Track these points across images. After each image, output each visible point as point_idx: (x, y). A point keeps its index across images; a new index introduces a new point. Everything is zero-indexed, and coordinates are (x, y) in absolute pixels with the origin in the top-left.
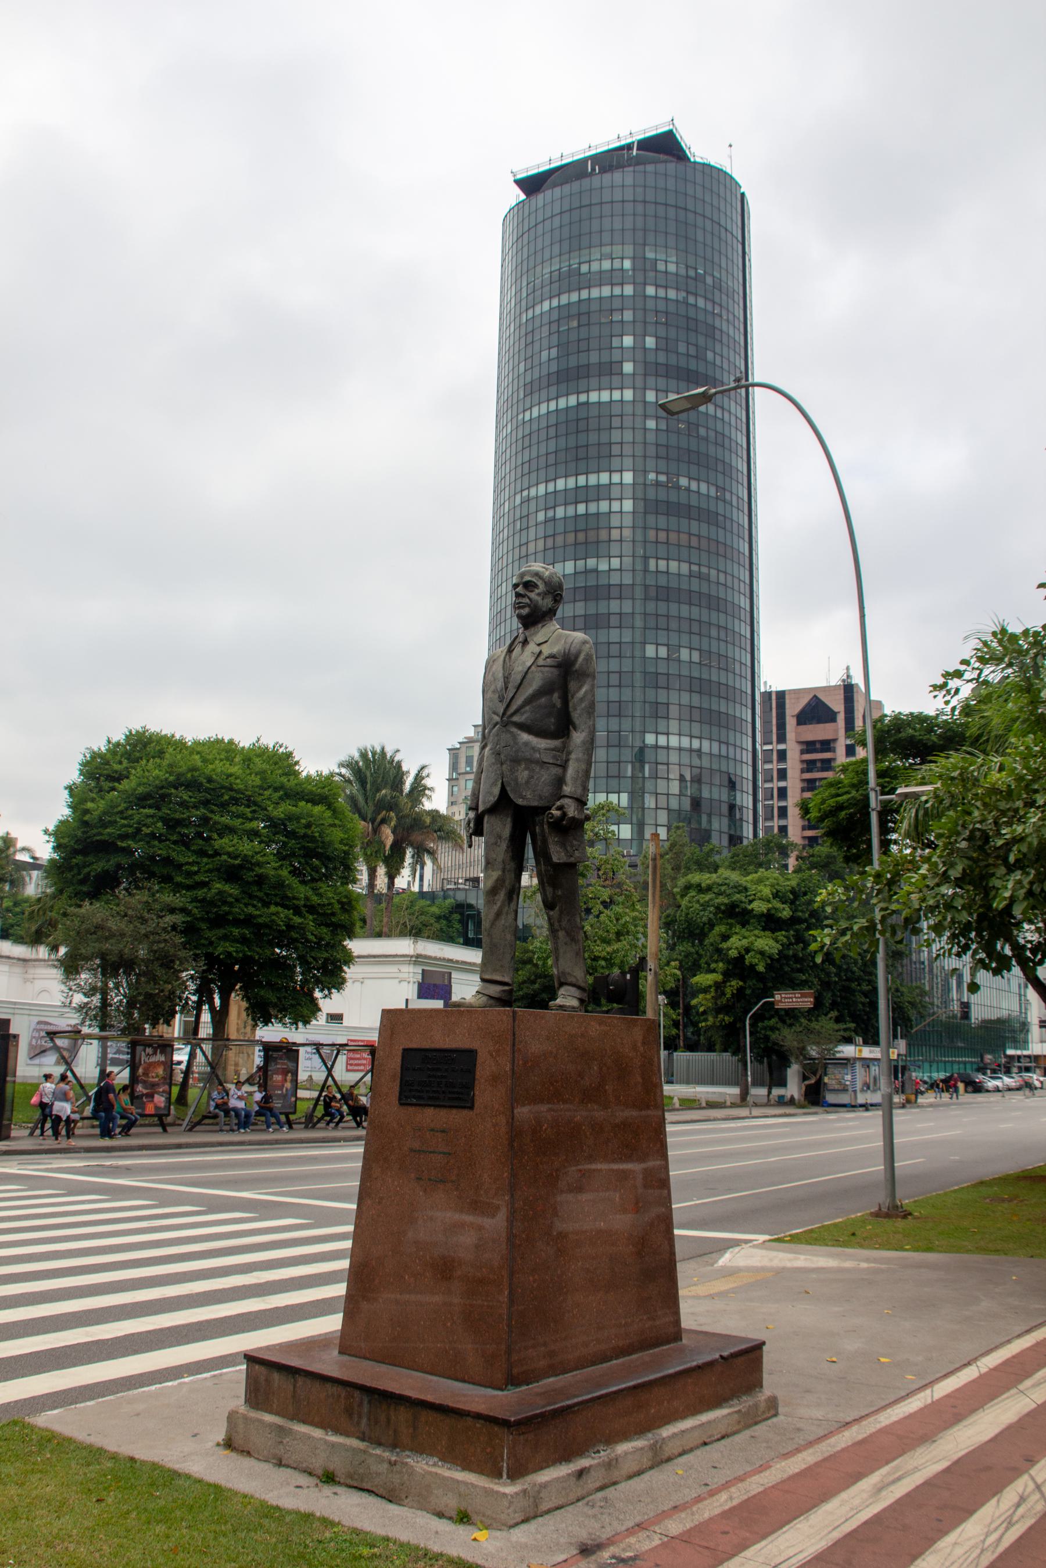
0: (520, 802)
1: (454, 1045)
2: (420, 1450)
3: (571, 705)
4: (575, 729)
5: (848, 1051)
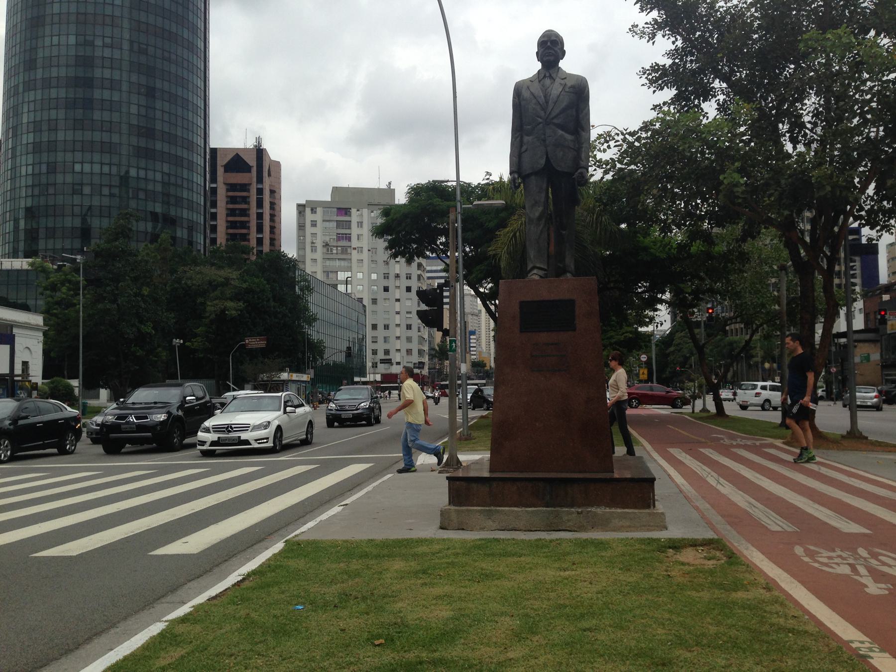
0: (559, 169)
1: (557, 298)
5: (285, 376)
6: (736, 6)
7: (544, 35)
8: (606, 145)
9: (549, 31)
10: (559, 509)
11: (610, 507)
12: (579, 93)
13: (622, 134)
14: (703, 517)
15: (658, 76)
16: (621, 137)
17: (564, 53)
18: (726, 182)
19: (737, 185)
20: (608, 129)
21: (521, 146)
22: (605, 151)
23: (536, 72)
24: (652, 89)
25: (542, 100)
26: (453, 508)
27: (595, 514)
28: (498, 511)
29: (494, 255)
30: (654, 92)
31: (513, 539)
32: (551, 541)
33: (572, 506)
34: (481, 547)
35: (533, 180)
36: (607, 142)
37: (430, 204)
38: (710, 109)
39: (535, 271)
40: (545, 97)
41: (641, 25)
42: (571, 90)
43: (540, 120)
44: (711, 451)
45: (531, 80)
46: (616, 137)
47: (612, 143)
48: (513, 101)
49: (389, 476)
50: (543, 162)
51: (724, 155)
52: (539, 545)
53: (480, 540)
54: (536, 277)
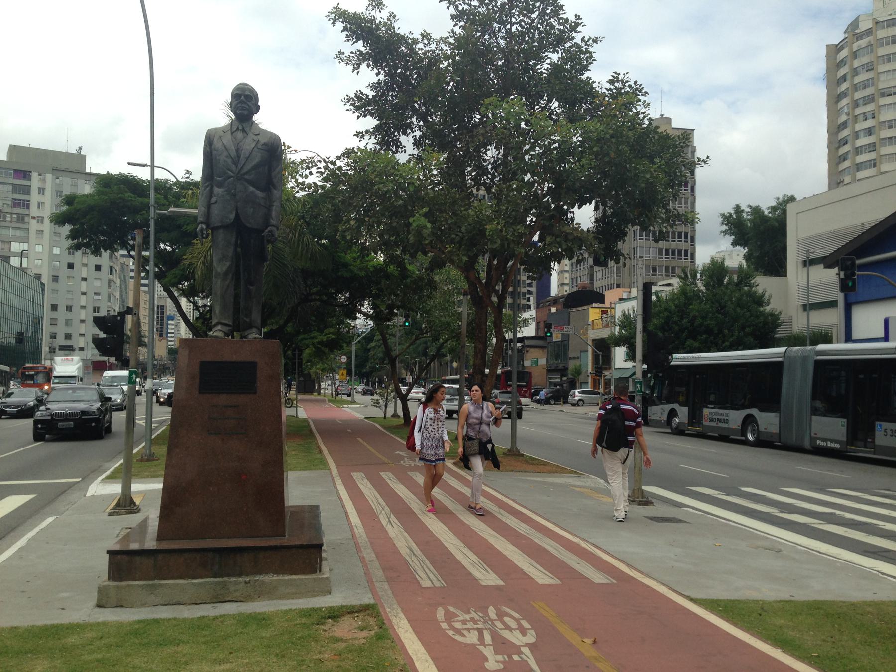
0: (248, 225)
1: (239, 360)
2: (260, 573)
3: (273, 174)
4: (275, 188)
6: (433, 52)
8: (308, 171)
9: (244, 84)
10: (226, 579)
11: (278, 574)
13: (324, 161)
14: (367, 574)
15: (360, 104)
16: (323, 165)
17: (258, 108)
18: (414, 225)
19: (425, 227)
20: (310, 155)
21: (211, 197)
22: (306, 177)
24: (357, 114)
25: (233, 154)
26: (112, 583)
27: (263, 582)
28: (161, 585)
29: (190, 265)
30: (358, 117)
31: (175, 619)
32: (215, 618)
33: (240, 575)
34: (140, 630)
35: (221, 235)
37: (120, 198)
38: (407, 141)
39: (219, 327)
40: (237, 150)
41: (347, 53)
44: (391, 475)
45: (223, 130)
46: (318, 164)
47: (314, 170)
48: (204, 149)
49: (50, 519)
50: (232, 216)
51: (417, 197)
52: (201, 624)
53: (140, 622)
54: (220, 334)
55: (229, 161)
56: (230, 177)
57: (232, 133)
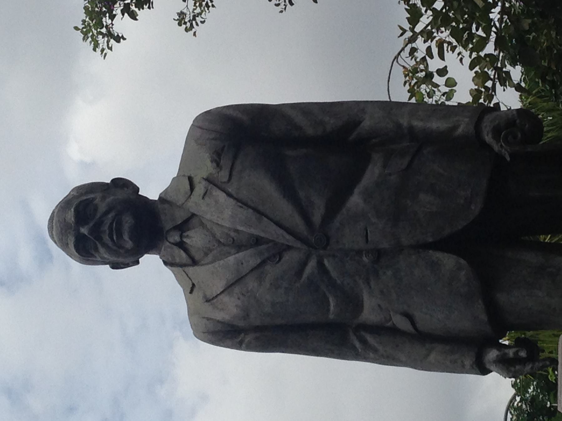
0: (476, 208)
3: (310, 131)
7: (64, 246)
8: (437, 79)
12: (238, 137)
16: (421, 44)
21: (394, 331)
22: (451, 83)
23: (168, 273)
25: (248, 258)
35: (512, 299)
36: (429, 76)
40: (239, 247)
42: (226, 162)
43: (312, 264)
46: (420, 55)
47: (435, 64)
50: (448, 261)
55: (272, 271)
56: (320, 264)
57: (194, 262)
